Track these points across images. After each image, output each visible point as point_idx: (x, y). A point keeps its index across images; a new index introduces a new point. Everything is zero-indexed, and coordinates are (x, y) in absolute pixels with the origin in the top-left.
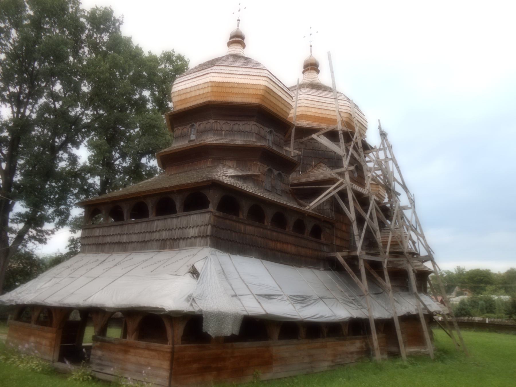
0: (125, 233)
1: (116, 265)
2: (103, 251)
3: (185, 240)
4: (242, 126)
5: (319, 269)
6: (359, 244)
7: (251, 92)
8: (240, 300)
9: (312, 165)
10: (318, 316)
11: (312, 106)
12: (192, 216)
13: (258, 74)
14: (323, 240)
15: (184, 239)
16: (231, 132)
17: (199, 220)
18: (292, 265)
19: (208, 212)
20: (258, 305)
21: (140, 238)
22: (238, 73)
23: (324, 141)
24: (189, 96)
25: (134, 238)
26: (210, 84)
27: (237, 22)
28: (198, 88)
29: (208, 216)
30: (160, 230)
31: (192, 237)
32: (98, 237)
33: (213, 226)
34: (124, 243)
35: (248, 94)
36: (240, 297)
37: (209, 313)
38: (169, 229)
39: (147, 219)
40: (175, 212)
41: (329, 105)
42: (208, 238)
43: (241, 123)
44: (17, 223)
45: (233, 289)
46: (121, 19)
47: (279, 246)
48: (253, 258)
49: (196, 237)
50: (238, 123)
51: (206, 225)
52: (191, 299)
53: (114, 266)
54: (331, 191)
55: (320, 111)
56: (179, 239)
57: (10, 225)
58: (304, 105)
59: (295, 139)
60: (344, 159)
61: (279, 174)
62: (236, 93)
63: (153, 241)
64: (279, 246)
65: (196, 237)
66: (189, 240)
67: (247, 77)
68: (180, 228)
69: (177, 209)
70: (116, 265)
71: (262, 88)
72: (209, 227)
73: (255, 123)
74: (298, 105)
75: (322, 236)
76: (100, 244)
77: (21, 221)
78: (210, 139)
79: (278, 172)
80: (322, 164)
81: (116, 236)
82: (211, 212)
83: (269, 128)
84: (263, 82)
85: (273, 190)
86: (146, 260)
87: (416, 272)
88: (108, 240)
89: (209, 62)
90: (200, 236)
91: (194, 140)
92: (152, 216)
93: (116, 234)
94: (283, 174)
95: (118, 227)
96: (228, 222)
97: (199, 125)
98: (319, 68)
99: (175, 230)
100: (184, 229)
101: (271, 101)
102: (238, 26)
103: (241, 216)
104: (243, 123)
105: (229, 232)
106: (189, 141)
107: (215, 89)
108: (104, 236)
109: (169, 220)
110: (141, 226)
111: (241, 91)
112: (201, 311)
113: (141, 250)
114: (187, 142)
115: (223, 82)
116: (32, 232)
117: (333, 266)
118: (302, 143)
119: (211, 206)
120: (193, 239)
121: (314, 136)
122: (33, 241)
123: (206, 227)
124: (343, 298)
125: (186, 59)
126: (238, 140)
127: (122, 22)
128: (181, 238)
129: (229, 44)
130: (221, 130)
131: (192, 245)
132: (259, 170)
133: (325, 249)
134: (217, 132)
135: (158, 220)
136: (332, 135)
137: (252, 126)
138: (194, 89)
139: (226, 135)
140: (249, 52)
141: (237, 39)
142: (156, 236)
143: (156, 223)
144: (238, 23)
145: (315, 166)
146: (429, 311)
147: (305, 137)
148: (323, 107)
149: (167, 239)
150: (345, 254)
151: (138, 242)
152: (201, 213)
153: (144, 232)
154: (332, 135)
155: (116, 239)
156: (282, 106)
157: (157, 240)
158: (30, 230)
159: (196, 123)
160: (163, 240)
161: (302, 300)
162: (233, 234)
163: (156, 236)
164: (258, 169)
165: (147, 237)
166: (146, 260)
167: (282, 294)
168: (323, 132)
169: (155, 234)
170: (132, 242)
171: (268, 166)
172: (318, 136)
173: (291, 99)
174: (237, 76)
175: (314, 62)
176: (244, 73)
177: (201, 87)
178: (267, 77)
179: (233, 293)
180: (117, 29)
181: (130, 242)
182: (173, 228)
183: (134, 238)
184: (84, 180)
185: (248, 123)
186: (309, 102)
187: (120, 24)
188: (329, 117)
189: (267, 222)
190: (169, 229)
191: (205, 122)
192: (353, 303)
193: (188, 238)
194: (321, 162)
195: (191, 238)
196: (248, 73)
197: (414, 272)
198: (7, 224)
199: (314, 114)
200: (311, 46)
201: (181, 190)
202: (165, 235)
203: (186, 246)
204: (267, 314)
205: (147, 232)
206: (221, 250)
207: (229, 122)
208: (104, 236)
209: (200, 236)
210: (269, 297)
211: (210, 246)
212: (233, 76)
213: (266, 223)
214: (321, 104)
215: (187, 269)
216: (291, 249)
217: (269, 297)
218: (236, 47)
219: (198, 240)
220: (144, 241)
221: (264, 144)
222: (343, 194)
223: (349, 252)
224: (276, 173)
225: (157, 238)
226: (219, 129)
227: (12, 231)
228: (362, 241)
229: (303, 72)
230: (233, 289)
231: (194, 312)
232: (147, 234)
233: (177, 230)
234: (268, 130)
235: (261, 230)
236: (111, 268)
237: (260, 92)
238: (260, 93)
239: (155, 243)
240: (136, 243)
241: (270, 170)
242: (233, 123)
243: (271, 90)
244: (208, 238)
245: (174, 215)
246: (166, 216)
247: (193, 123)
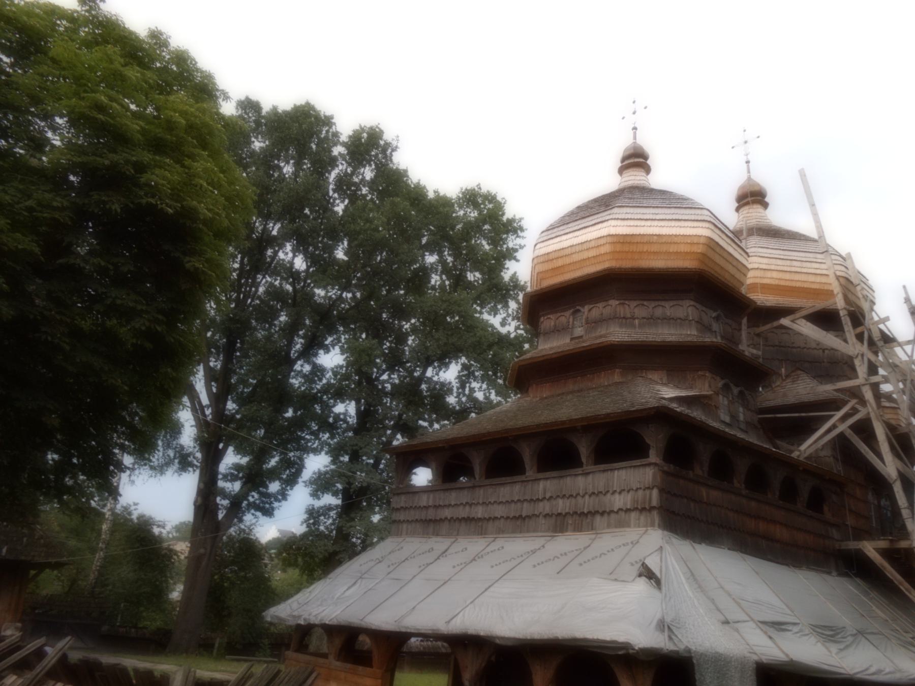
0: (481, 502)
1: (474, 559)
2: (437, 534)
3: (606, 515)
4: (669, 308)
5: (829, 573)
7: (682, 248)
8: (737, 630)
9: (780, 375)
10: (873, 670)
11: (773, 267)
12: (616, 472)
13: (693, 217)
15: (603, 514)
16: (652, 320)
17: (635, 479)
18: (787, 565)
19: (649, 465)
21: (513, 510)
22: (658, 217)
23: (808, 330)
24: (567, 261)
25: (499, 511)
26: (609, 240)
27: (632, 132)
28: (585, 246)
30: (551, 497)
31: (620, 509)
33: (662, 491)
34: (480, 519)
35: (677, 253)
36: (736, 625)
37: (702, 654)
38: (571, 496)
39: (523, 478)
40: (579, 464)
41: (805, 264)
42: (655, 513)
43: (667, 304)
45: (719, 610)
46: (394, 143)
48: (726, 551)
49: (628, 511)
50: (663, 303)
51: (648, 488)
53: (471, 562)
55: (788, 276)
56: (593, 513)
57: (221, 484)
61: (741, 393)
62: (655, 253)
63: (538, 516)
65: (628, 511)
66: (613, 516)
67: (673, 223)
68: (593, 493)
69: (584, 460)
70: (474, 559)
71: (702, 241)
72: (655, 492)
73: (692, 303)
75: (826, 508)
76: (431, 520)
78: (618, 334)
79: (739, 389)
80: (799, 372)
81: (461, 508)
82: (655, 464)
83: (715, 311)
84: (703, 231)
86: (534, 552)
88: (447, 513)
89: (596, 201)
90: (636, 509)
91: (581, 337)
92: (530, 473)
93: (462, 504)
94: (746, 392)
95: (466, 492)
97: (590, 310)
98: (767, 199)
99: (583, 496)
100: (601, 496)
101: (716, 263)
102: (635, 138)
104: (672, 303)
105: (685, 500)
106: (572, 339)
107: (618, 248)
109: (569, 480)
110: (510, 490)
111: (664, 248)
112: (689, 651)
113: (514, 532)
114: (568, 340)
115: (633, 235)
116: (253, 497)
117: (856, 567)
118: (758, 335)
119: (652, 453)
120: (622, 514)
121: (785, 321)
122: (252, 511)
123: (648, 492)
125: (499, 198)
127: (397, 147)
128: (597, 512)
129: (621, 171)
130: (633, 318)
131: (622, 524)
132: (710, 386)
133: (835, 533)
134: (626, 321)
135: (547, 479)
136: (826, 319)
137: (686, 308)
138: (578, 249)
139: (641, 326)
140: (658, 179)
141: (636, 159)
143: (542, 484)
144: (635, 134)
145: (787, 376)
147: (765, 324)
148: (793, 269)
149: (567, 514)
150: (883, 544)
151: (508, 518)
152: (635, 467)
153: (519, 500)
155: (463, 512)
156: (732, 271)
157: (546, 516)
159: (583, 307)
160: (559, 514)
164: (707, 385)
165: (526, 509)
166: (534, 552)
167: (798, 621)
168: (804, 313)
169: (541, 504)
170: (496, 518)
171: (722, 379)
172: (793, 321)
173: (745, 256)
174: (656, 223)
175: (756, 189)
176: (668, 217)
177: (593, 244)
178: (709, 222)
179: (723, 618)
180: (388, 158)
181: (490, 518)
182: (578, 494)
183: (499, 511)
184: (327, 408)
185: (680, 302)
186: (765, 261)
187: (393, 150)
188: (806, 285)
190: (571, 496)
191: (601, 305)
193: (612, 511)
194: (799, 369)
195: (617, 512)
196: (674, 217)
198: (216, 483)
199: (777, 282)
200: (748, 162)
201: (589, 426)
202: (562, 505)
203: (609, 526)
204: (792, 663)
205: (526, 500)
206: (677, 534)
207: (645, 303)
209: (637, 508)
210: (778, 626)
211: (659, 527)
212: (649, 223)
213: (736, 484)
214: (788, 263)
216: (781, 533)
217: (778, 626)
218: (635, 173)
219: (633, 515)
220: (520, 516)
221: (708, 339)
222: (864, 429)
223: (891, 541)
224: (736, 390)
225: (547, 510)
226: (629, 315)
227: (224, 494)
229: (737, 210)
230: (719, 610)
231: (677, 652)
232: (525, 505)
233: (587, 497)
234: (714, 315)
236: (466, 564)
237: (700, 249)
238: (699, 251)
240: (502, 520)
241: (726, 387)
242: (653, 304)
243: (717, 243)
244: (655, 513)
245: (579, 471)
246: (563, 473)
247: (578, 307)
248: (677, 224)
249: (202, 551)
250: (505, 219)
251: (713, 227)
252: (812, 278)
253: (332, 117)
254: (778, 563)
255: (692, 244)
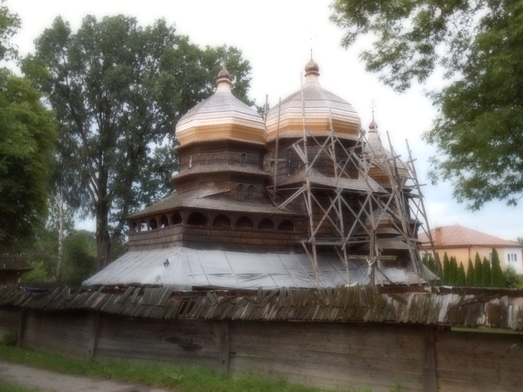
2: (138, 250)
4: (219, 155)
6: (313, 233)
7: (223, 129)
11: (296, 117)
13: (226, 116)
14: (295, 231)
16: (212, 162)
17: (177, 231)
20: (206, 280)
22: (212, 117)
29: (181, 227)
32: (136, 241)
33: (184, 234)
44: (114, 221)
47: (244, 240)
48: (219, 251)
49: (176, 241)
52: (159, 278)
54: (301, 190)
58: (290, 117)
59: (279, 149)
60: (306, 166)
62: (213, 132)
64: (244, 240)
65: (176, 241)
67: (218, 119)
71: (230, 126)
73: (228, 152)
74: (280, 120)
77: (117, 220)
78: (198, 169)
85: (247, 199)
87: (382, 251)
88: (140, 243)
96: (196, 230)
103: (208, 225)
104: (220, 153)
108: (139, 240)
119: (182, 221)
124: (300, 274)
125: (238, 50)
126: (216, 168)
130: (205, 160)
131: (175, 246)
134: (202, 162)
137: (226, 154)
139: (208, 164)
142: (160, 240)
145: (301, 168)
146: (391, 282)
154: (301, 144)
155: (144, 242)
157: (161, 243)
158: (124, 226)
159: (191, 155)
161: (251, 276)
162: (201, 237)
163: (160, 240)
165: (157, 241)
174: (211, 120)
176: (216, 116)
177: (190, 130)
179: (190, 274)
183: (152, 241)
186: (293, 114)
188: (311, 124)
189: (233, 226)
191: (196, 155)
192: (308, 278)
196: (219, 116)
197: (379, 250)
199: (298, 124)
202: (164, 239)
208: (139, 240)
210: (219, 275)
212: (209, 120)
215: (164, 261)
216: (259, 241)
217: (219, 275)
227: (110, 228)
228: (316, 231)
234: (241, 154)
235: (226, 232)
239: (160, 245)
242: (213, 154)
243: (239, 125)
248: (220, 119)
249: (103, 257)
250: (240, 63)
251: (235, 119)
252: (314, 121)
253: (135, 18)
254: (260, 253)
255: (226, 127)
